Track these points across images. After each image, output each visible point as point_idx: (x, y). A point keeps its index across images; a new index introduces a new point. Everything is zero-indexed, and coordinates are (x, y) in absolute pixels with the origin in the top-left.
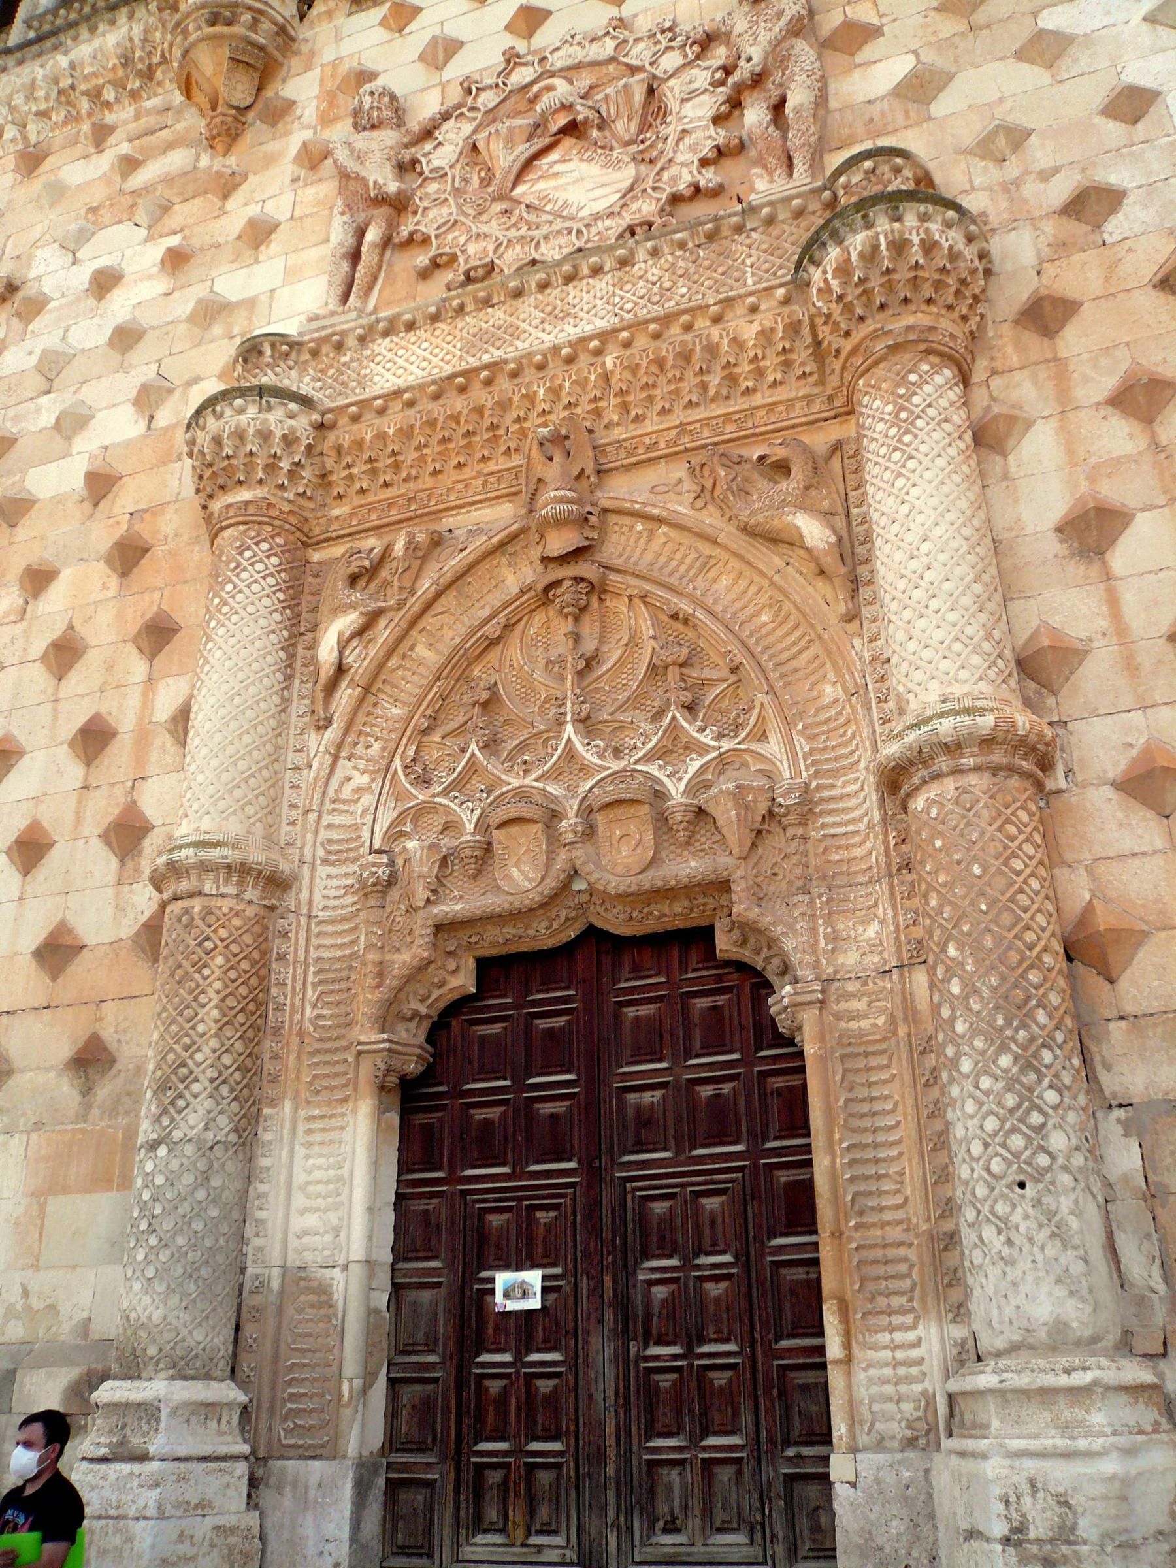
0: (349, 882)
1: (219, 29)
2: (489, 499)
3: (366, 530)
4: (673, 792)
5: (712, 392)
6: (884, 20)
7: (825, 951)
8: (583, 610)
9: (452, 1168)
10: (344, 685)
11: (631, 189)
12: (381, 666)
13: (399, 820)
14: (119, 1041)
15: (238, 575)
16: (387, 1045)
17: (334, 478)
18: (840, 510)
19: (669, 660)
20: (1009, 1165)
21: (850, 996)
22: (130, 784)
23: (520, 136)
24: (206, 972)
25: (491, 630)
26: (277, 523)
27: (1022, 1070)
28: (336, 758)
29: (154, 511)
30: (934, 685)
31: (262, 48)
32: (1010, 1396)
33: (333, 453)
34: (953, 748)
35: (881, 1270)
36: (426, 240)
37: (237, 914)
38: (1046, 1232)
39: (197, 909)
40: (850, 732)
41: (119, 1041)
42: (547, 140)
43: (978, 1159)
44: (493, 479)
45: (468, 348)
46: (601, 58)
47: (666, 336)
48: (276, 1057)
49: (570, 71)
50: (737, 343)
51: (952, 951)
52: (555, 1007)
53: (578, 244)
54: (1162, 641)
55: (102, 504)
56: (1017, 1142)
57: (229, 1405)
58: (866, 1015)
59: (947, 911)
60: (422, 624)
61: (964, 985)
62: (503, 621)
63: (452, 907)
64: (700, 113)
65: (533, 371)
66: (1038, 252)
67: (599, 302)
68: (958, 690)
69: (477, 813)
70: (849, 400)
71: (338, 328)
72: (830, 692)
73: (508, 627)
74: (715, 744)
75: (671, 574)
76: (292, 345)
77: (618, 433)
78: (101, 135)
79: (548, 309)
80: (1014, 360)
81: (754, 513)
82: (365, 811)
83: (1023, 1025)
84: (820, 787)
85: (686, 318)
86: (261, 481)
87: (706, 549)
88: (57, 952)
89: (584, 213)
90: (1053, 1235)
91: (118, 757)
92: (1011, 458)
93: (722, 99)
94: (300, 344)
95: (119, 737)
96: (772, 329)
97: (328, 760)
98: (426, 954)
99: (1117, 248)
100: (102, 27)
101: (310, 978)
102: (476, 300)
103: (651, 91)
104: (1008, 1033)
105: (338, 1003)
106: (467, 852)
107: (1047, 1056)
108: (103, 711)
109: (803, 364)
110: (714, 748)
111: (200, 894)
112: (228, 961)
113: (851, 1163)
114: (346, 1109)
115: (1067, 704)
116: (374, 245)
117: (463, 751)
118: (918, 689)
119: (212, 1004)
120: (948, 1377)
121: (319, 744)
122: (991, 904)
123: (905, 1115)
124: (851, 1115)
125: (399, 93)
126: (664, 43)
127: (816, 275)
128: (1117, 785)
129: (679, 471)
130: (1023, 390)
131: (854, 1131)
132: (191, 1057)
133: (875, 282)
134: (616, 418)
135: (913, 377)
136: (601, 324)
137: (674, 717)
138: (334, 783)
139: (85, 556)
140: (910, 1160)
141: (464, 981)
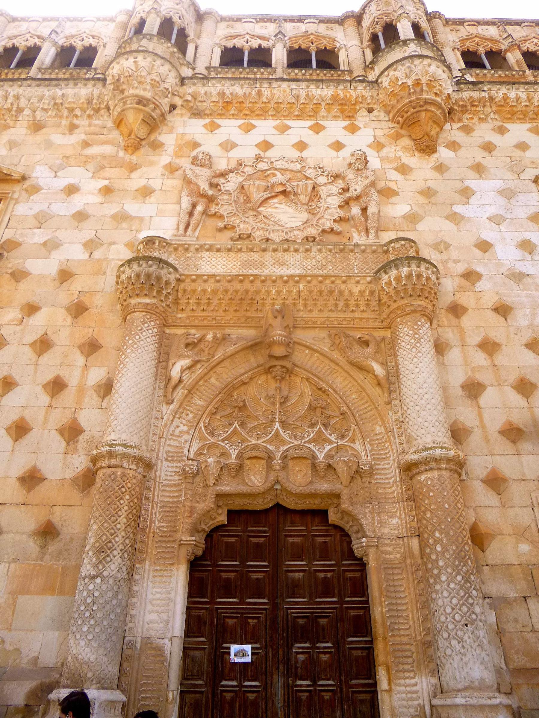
0: (178, 470)
1: (140, 107)
4: (319, 457)
5: (340, 308)
7: (377, 527)
8: (283, 378)
9: (212, 597)
10: (180, 387)
11: (306, 222)
12: (197, 383)
13: (202, 448)
14: (62, 525)
15: (141, 333)
16: (194, 543)
17: (181, 302)
18: (385, 362)
19: (319, 405)
20: (462, 617)
21: (387, 545)
22: (74, 409)
23: (262, 189)
24: (122, 501)
26: (158, 315)
27: (465, 582)
28: (174, 417)
29: (92, 293)
30: (429, 436)
31: (155, 119)
32: (468, 707)
33: (182, 292)
34: (437, 460)
35: (400, 654)
36: (221, 217)
37: (135, 478)
38: (476, 644)
39: (119, 473)
40: (386, 446)
41: (62, 525)
42: (274, 194)
43: (449, 614)
44: (250, 319)
45: (244, 265)
47: (324, 283)
48: (142, 542)
49: (283, 171)
50: (351, 293)
51: (437, 534)
52: (259, 534)
53: (286, 237)
54: (497, 433)
55: (65, 284)
56: (465, 609)
57: (119, 702)
58: (393, 553)
59: (435, 520)
60: (215, 370)
61: (442, 548)
62: (250, 376)
63: (225, 487)
64: (334, 202)
65: (270, 282)
66: (454, 288)
67: (298, 263)
68: (438, 439)
69: (237, 451)
70: (390, 324)
71: (188, 242)
72: (379, 429)
73: (251, 379)
75: (319, 372)
76: (167, 243)
77: (301, 314)
78: (72, 128)
79: (277, 260)
80: (446, 323)
81: (357, 357)
82: (186, 442)
83: (465, 565)
84: (375, 464)
85: (333, 278)
86: (154, 297)
87: (333, 366)
88: (31, 479)
89: (287, 226)
90: (479, 645)
91: (68, 398)
93: (342, 200)
94: (170, 244)
95: (69, 388)
96: (364, 291)
97: (171, 417)
98: (213, 506)
99: (480, 293)
100: (80, 85)
101: (158, 509)
102: (247, 248)
103: (314, 188)
104: (460, 567)
105: (171, 521)
106: (233, 467)
107: (472, 577)
108: (62, 374)
109: (374, 306)
110: (335, 443)
111: (121, 467)
112: (130, 498)
113: (390, 610)
114: (174, 568)
116: (199, 212)
117: (231, 425)
118: (422, 436)
119: (124, 516)
120: (435, 696)
121: (167, 410)
122: (453, 518)
123: (410, 594)
124: (388, 591)
125: (213, 155)
126: (320, 173)
127: (385, 277)
129: (323, 334)
130: (449, 335)
131: (389, 597)
132: (114, 539)
133: (410, 287)
134: (302, 308)
135: (419, 323)
136: (298, 271)
137: (320, 428)
138: (172, 428)
139: (56, 304)
140: (412, 612)
141: (223, 519)
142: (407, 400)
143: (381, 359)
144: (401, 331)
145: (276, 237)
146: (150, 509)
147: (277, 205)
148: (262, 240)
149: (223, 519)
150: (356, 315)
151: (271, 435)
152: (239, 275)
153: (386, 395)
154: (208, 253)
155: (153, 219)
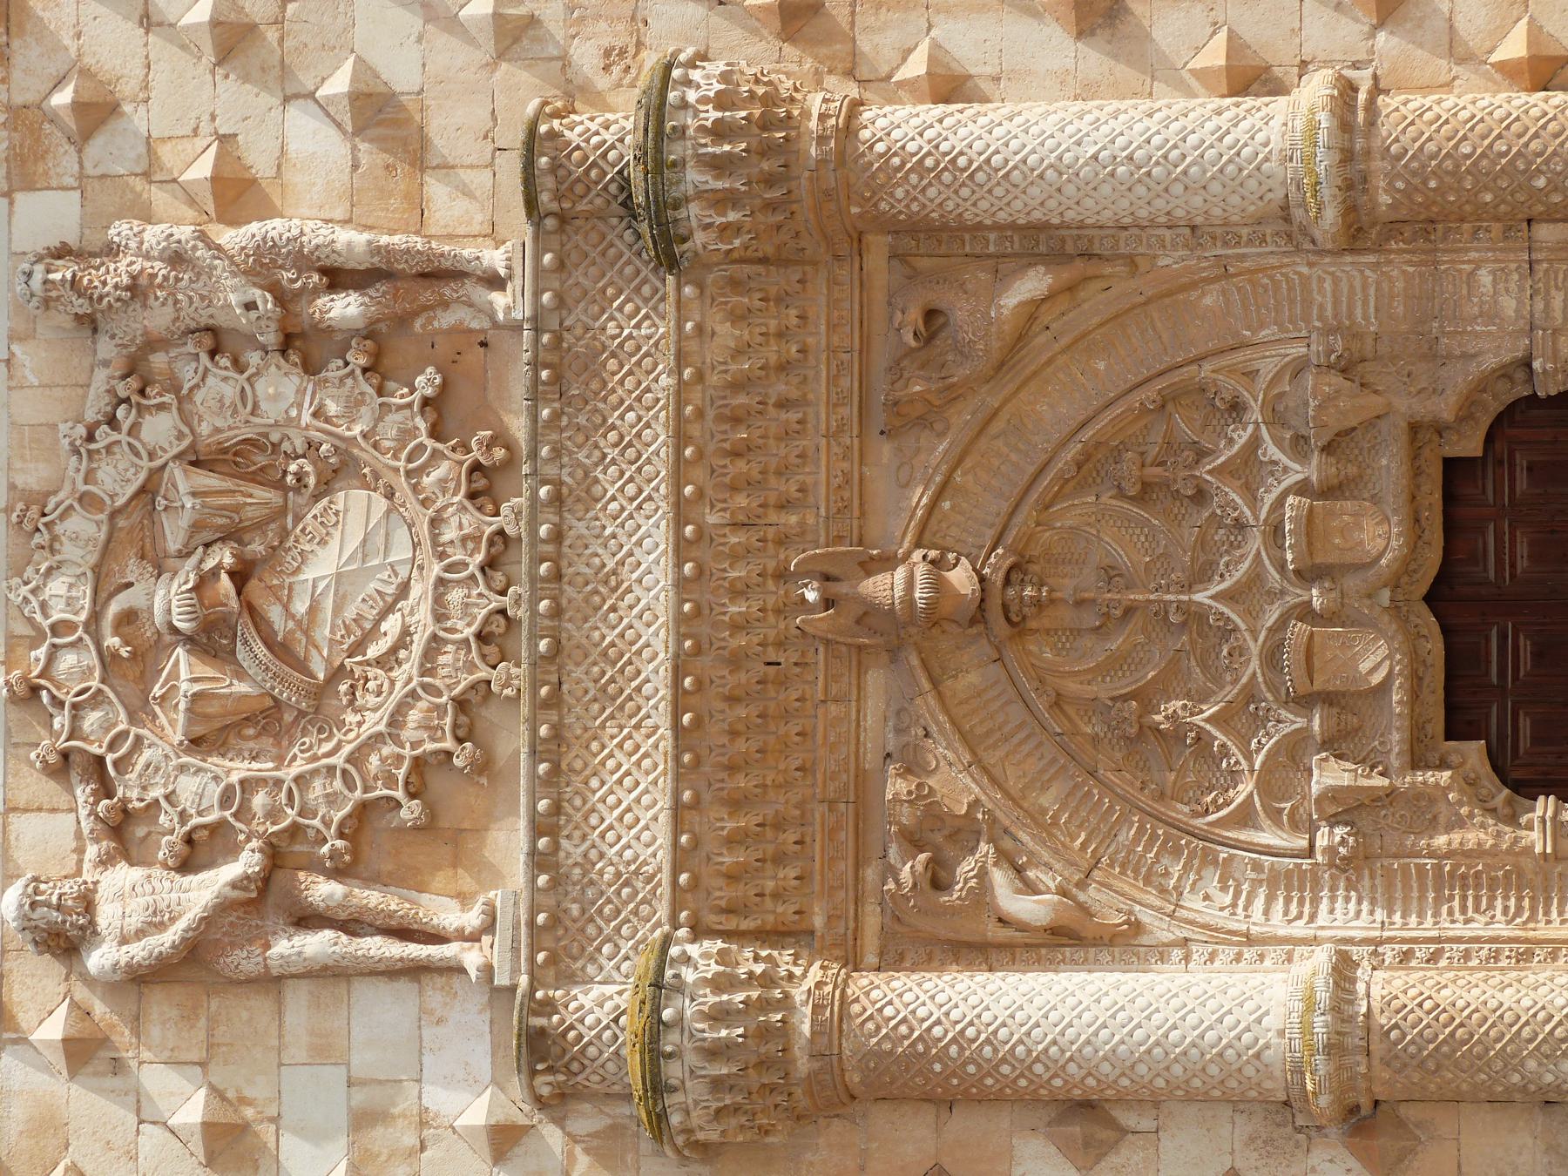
2: (858, 700)
3: (857, 878)
4: (1300, 477)
5: (794, 394)
6: (205, 127)
10: (1082, 897)
13: (1275, 816)
18: (991, 262)
19: (1136, 473)
21: (1547, 305)
25: (1041, 705)
40: (1266, 281)
44: (834, 689)
46: (103, 536)
62: (1036, 684)
69: (1284, 713)
74: (1250, 428)
82: (1257, 867)
87: (998, 425)
92: (973, 71)
103: (194, 464)
115: (1281, 58)
118: (1265, 188)
127: (699, 238)
128: (1380, 25)
137: (1209, 472)
141: (1473, 752)
142: (1143, 213)
143: (982, 276)
144: (900, 207)
145: (473, 606)
146: (1463, 947)
147: (300, 607)
148: (483, 657)
149: (1473, 752)
150: (817, 338)
151: (1234, 616)
152: (676, 726)
153: (1108, 270)
154: (564, 843)
155: (356, 1072)
